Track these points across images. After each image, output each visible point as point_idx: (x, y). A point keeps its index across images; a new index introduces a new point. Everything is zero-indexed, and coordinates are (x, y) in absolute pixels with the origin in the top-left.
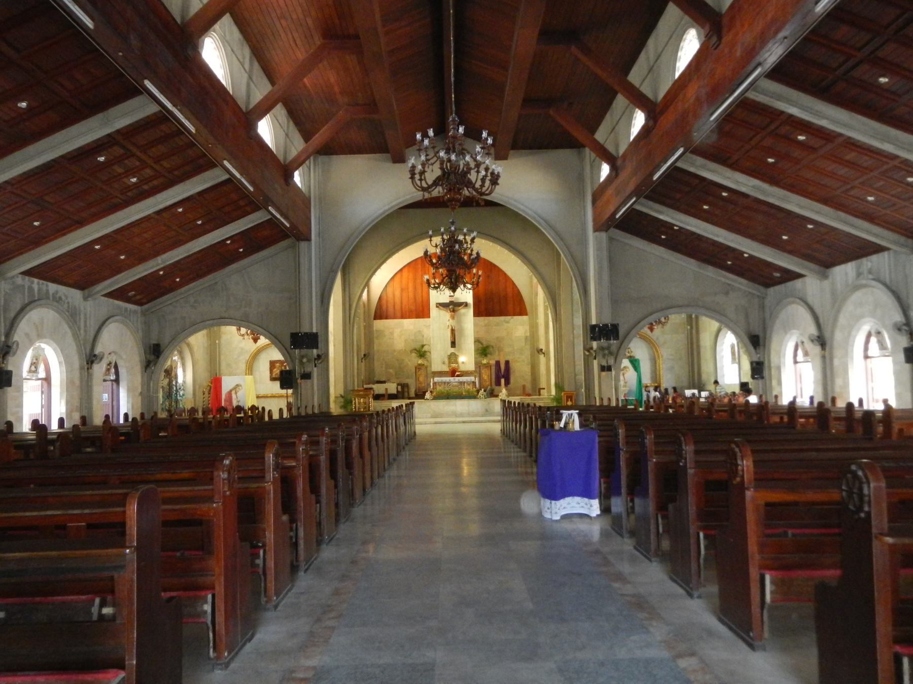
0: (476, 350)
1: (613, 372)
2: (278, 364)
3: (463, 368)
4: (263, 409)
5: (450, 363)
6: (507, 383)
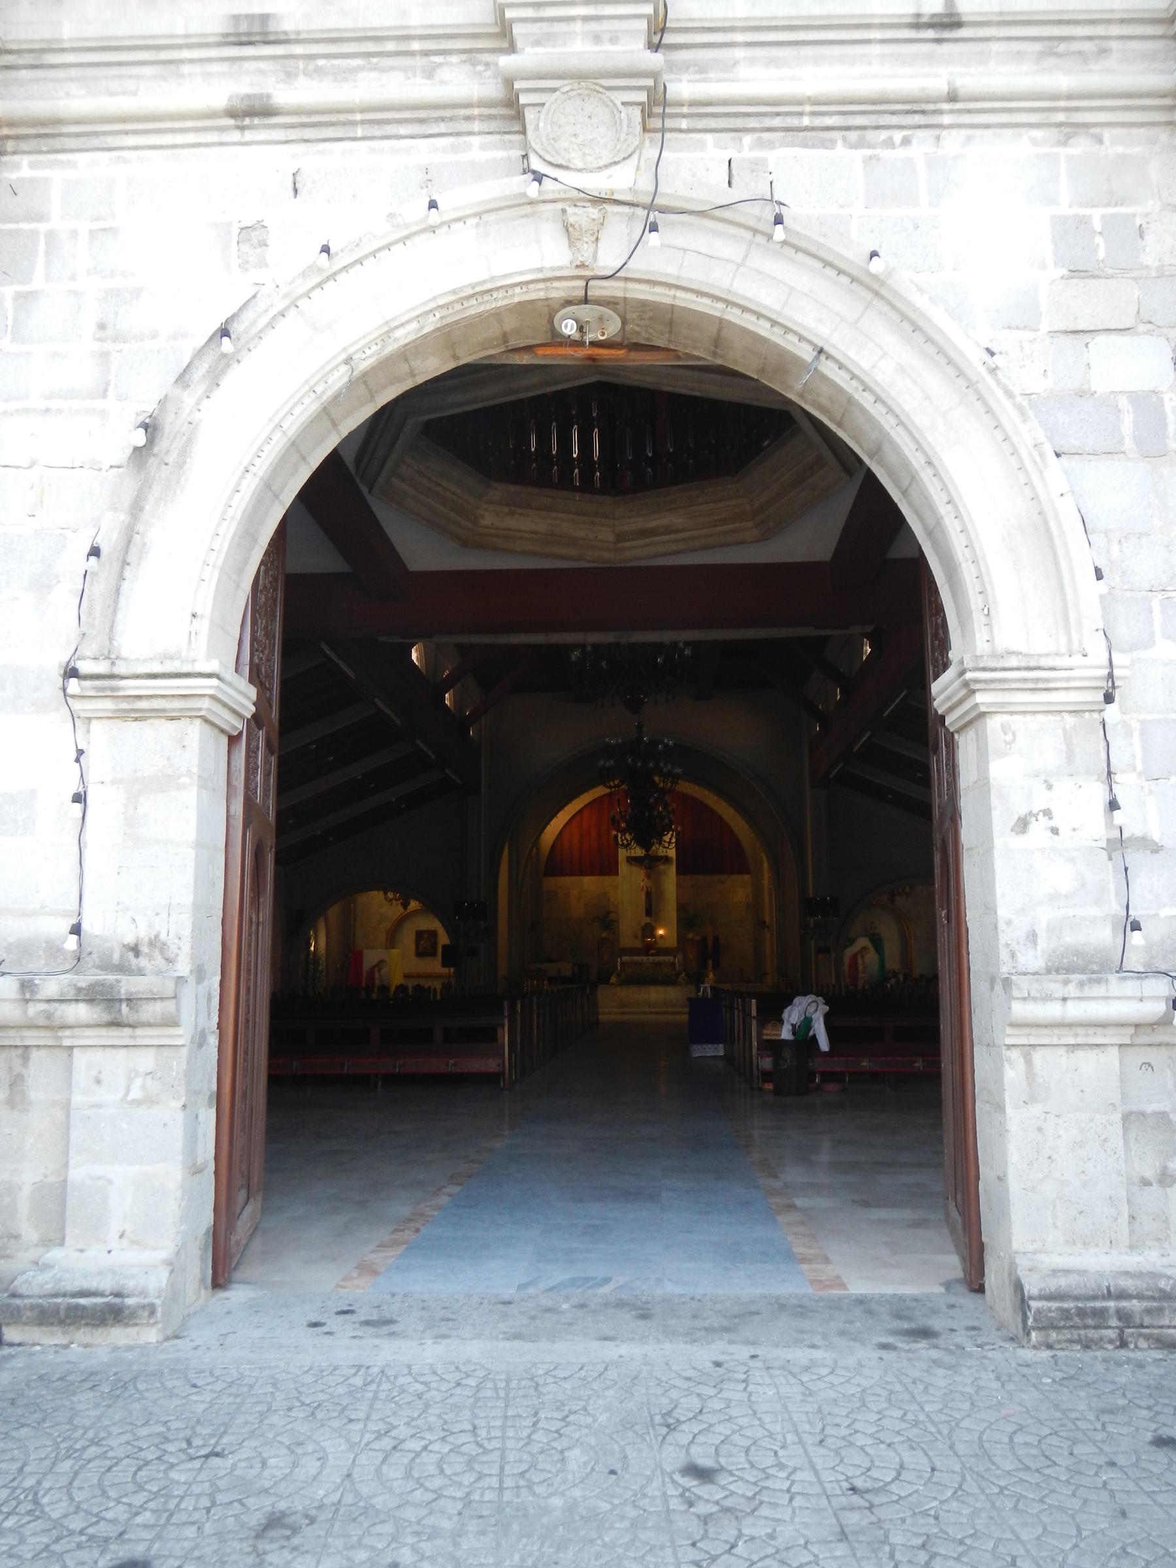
0: (679, 920)
1: (833, 955)
2: (426, 936)
3: (661, 944)
4: (429, 988)
5: (644, 936)
6: (716, 966)
